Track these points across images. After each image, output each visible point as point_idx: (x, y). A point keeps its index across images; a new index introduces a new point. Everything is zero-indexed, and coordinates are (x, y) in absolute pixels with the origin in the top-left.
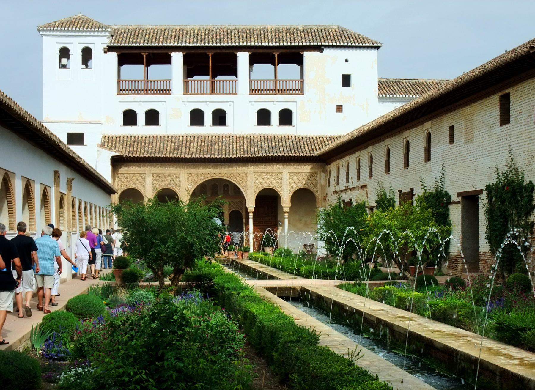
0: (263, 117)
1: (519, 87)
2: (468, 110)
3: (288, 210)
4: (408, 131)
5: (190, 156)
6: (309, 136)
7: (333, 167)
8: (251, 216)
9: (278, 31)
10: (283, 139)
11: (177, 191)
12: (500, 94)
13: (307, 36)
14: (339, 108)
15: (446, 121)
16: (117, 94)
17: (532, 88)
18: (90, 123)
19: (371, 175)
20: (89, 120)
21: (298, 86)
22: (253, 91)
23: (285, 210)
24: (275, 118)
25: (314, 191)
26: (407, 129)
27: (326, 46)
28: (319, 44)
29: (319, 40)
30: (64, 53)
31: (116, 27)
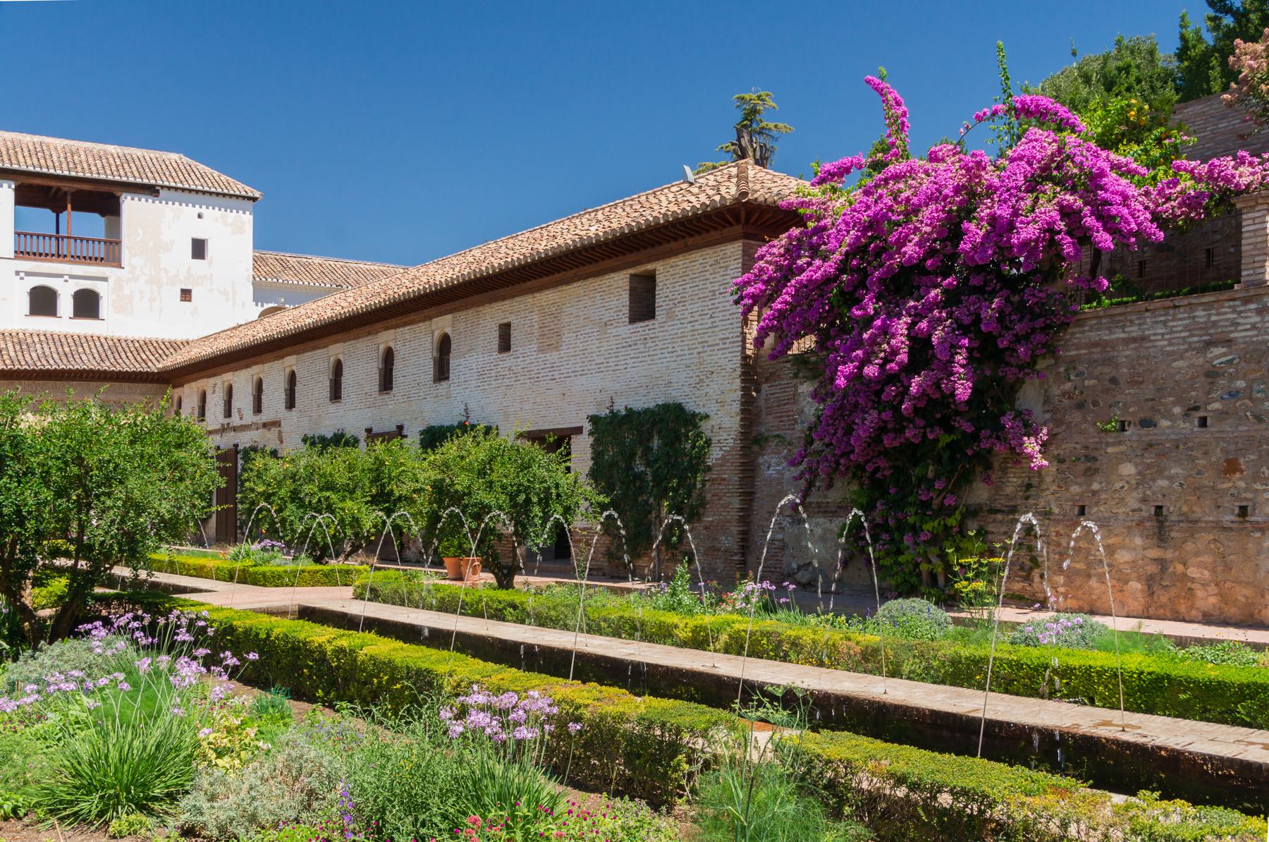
0: (43, 301)
1: (680, 262)
2: (548, 297)
4: (391, 332)
6: (130, 337)
7: (189, 393)
10: (83, 340)
12: (631, 271)
13: (126, 166)
14: (186, 294)
15: (490, 316)
17: (712, 261)
19: (291, 404)
21: (100, 251)
22: (20, 254)
24: (65, 304)
26: (387, 328)
27: (163, 187)
28: (153, 182)
29: (150, 175)
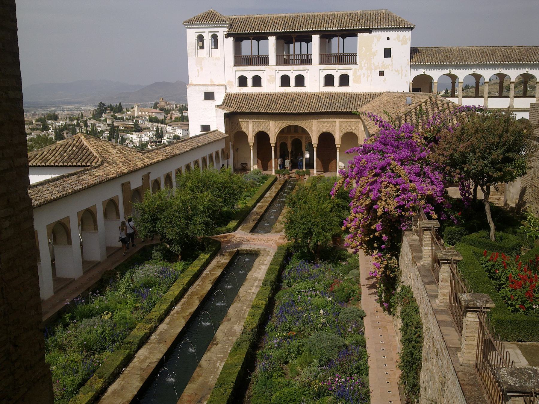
0: (329, 80)
3: (339, 146)
5: (275, 112)
8: (315, 150)
9: (343, 17)
11: (268, 133)
14: (381, 73)
16: (235, 66)
18: (217, 86)
20: (216, 83)
23: (337, 146)
24: (337, 81)
25: (357, 134)
27: (373, 29)
29: (368, 24)
30: (201, 38)
31: (235, 17)
